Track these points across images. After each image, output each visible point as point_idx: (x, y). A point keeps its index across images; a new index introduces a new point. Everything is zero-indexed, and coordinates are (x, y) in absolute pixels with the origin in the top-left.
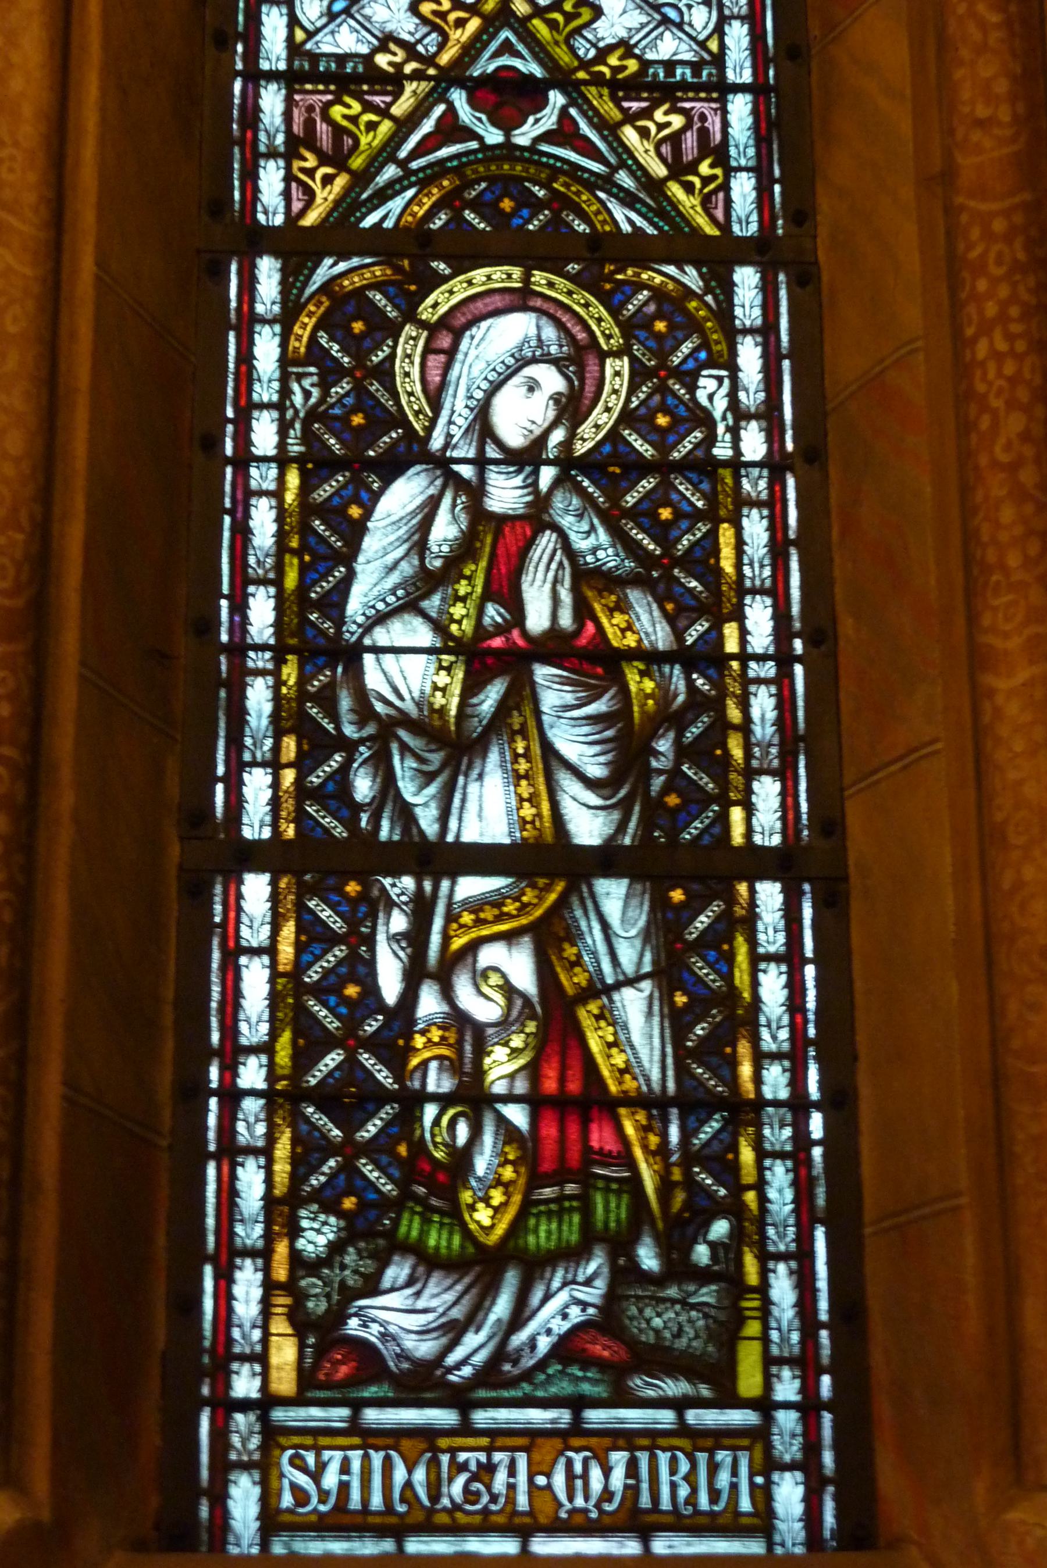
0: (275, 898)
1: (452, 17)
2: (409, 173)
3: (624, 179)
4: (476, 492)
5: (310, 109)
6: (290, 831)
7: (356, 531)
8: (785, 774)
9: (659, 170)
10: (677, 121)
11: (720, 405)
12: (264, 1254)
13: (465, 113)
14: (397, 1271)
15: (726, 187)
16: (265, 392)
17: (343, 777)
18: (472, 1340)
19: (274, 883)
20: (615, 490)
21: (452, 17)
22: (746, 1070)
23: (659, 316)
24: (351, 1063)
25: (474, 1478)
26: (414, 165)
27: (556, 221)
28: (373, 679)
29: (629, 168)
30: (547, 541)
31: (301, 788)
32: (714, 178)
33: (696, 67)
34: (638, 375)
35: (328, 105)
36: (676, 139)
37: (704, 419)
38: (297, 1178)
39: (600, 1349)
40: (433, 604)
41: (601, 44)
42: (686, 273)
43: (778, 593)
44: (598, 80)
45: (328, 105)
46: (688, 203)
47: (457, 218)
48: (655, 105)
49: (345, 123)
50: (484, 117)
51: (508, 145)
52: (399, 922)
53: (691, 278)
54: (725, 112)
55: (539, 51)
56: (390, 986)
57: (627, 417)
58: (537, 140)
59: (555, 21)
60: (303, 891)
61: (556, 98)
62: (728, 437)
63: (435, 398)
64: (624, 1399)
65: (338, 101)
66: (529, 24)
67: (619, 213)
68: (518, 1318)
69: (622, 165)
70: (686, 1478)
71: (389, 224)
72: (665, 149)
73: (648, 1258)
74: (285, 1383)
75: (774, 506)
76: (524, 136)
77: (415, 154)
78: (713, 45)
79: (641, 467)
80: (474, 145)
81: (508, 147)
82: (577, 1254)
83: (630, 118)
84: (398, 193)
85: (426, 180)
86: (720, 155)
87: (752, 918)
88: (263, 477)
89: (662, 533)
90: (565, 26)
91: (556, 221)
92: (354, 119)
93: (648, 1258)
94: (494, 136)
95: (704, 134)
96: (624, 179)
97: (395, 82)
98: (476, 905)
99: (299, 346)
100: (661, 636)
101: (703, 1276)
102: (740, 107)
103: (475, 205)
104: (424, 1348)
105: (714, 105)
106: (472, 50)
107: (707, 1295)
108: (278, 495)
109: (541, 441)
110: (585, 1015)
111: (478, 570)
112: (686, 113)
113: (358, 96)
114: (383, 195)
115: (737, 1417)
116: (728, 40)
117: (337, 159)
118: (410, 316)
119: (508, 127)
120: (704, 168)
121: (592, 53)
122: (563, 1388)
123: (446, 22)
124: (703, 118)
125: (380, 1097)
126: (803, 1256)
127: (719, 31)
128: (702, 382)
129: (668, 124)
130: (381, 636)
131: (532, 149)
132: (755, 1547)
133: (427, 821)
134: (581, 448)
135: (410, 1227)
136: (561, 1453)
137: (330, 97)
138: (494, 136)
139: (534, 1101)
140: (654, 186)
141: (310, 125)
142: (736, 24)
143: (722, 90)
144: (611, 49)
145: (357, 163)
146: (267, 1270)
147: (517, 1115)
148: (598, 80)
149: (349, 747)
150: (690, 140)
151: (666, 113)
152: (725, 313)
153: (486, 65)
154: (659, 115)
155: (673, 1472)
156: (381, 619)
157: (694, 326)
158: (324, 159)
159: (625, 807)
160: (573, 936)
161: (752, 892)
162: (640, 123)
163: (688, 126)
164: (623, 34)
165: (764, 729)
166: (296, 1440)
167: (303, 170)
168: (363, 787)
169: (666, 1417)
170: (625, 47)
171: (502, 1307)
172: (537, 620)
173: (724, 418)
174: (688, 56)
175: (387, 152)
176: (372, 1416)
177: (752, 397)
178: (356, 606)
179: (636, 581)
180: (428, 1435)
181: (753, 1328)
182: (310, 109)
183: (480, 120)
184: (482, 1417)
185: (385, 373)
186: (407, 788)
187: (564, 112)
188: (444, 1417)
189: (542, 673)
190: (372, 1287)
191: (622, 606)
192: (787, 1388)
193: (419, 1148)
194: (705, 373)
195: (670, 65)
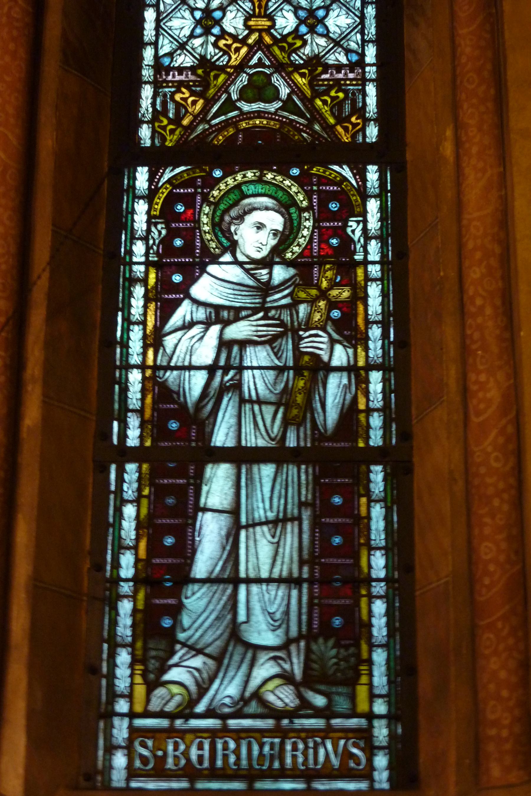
5: (165, 95)
11: (358, 233)
26: (214, 122)
35: (173, 94)
42: (343, 169)
45: (173, 94)
53: (346, 172)
59: (284, 47)
62: (362, 249)
65: (179, 91)
66: (271, 49)
72: (335, 110)
86: (361, 112)
90: (289, 49)
92: (185, 99)
113: (188, 87)
115: (353, 722)
128: (350, 224)
137: (173, 90)
141: (164, 104)
142: (370, 45)
158: (171, 121)
162: (323, 98)
163: (346, 97)
181: (364, 679)
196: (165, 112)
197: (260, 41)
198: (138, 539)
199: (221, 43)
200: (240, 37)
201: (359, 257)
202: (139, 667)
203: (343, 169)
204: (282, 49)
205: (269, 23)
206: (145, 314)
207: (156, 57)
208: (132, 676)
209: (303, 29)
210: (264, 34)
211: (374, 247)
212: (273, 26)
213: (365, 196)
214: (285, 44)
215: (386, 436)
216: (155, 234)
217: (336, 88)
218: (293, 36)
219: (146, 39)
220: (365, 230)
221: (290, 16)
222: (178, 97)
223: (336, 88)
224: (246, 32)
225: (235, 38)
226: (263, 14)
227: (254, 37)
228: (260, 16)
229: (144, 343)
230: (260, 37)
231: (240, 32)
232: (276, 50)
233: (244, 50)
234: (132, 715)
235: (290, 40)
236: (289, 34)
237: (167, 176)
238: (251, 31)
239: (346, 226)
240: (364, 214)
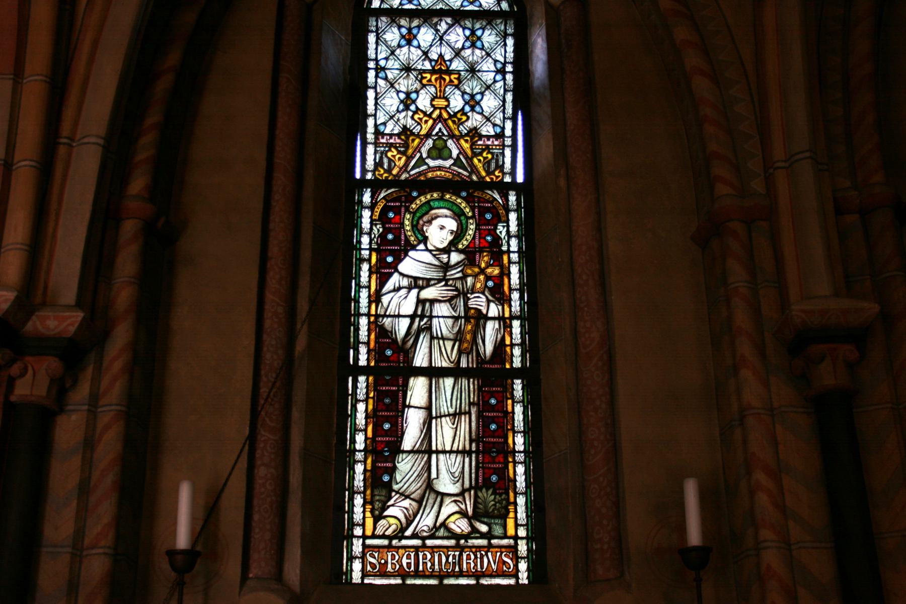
11: (504, 233)
42: (494, 193)
59: (455, 121)
62: (506, 244)
128: (499, 227)
167: (378, 174)
194: (499, 224)
197: (440, 116)
199: (416, 117)
200: (428, 113)
201: (505, 248)
202: (369, 507)
203: (494, 193)
204: (454, 122)
205: (446, 103)
206: (370, 281)
207: (376, 126)
208: (364, 512)
209: (467, 108)
211: (514, 243)
212: (448, 106)
213: (508, 210)
214: (455, 119)
215: (523, 361)
218: (461, 113)
219: (369, 112)
220: (508, 232)
221: (459, 98)
224: (432, 109)
225: (425, 113)
227: (437, 112)
229: (369, 300)
230: (441, 113)
231: (428, 109)
232: (450, 122)
233: (430, 122)
234: (364, 537)
235: (459, 116)
236: (459, 112)
238: (435, 108)
239: (496, 228)
240: (507, 221)
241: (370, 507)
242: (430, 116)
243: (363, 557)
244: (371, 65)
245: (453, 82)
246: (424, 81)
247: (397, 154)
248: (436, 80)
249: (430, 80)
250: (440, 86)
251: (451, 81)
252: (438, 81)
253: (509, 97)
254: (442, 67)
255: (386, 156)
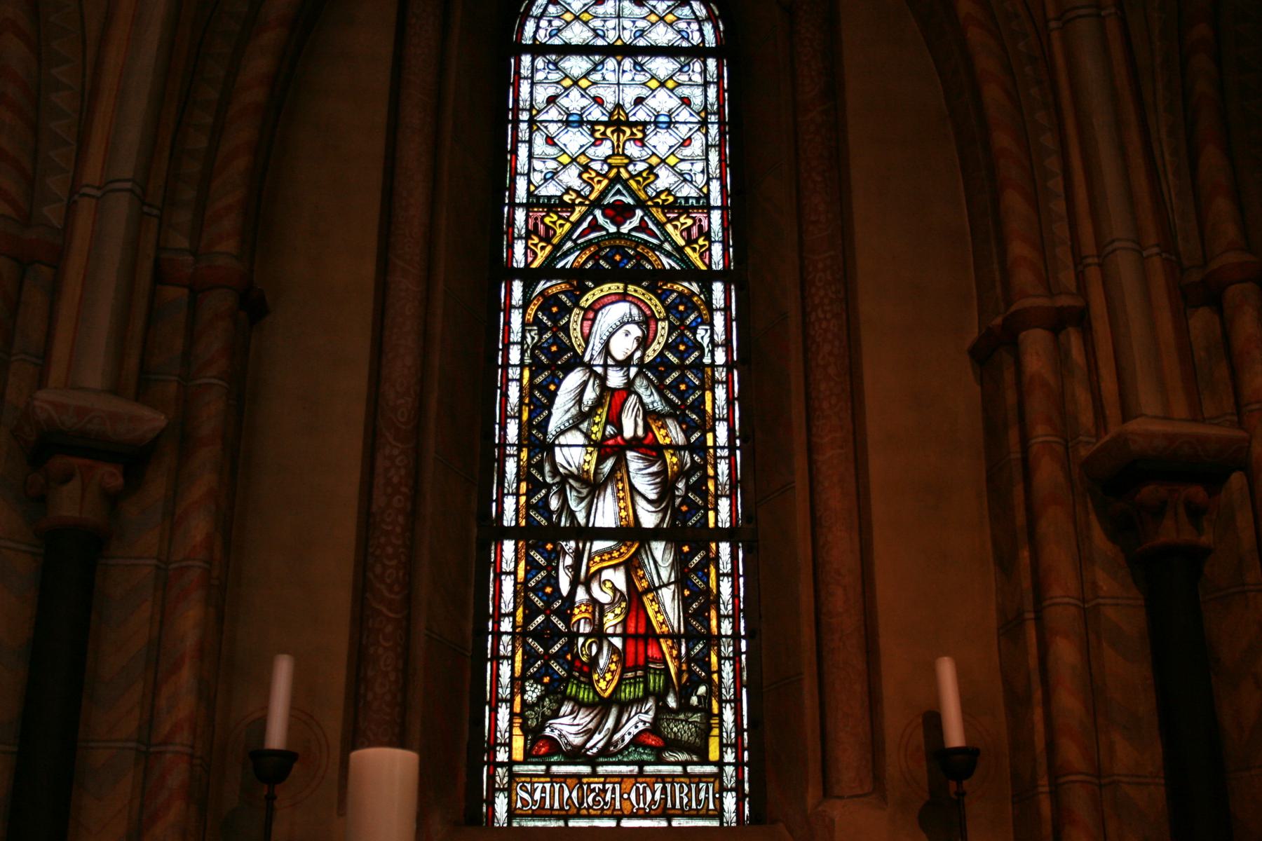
0: (516, 551)
1: (596, 180)
2: (576, 245)
3: (667, 246)
4: (603, 379)
5: (536, 219)
6: (523, 523)
7: (552, 396)
8: (732, 497)
9: (681, 242)
10: (690, 222)
11: (706, 341)
12: (511, 701)
13: (601, 220)
14: (567, 708)
15: (709, 249)
16: (516, 337)
17: (546, 500)
18: (597, 737)
19: (516, 544)
20: (661, 378)
21: (596, 180)
22: (714, 623)
23: (681, 303)
24: (548, 619)
25: (598, 795)
26: (579, 242)
27: (638, 264)
28: (559, 457)
29: (669, 242)
30: (633, 399)
31: (529, 506)
32: (705, 245)
33: (698, 199)
34: (672, 328)
35: (543, 217)
36: (689, 229)
37: (700, 347)
38: (525, 668)
39: (652, 741)
40: (584, 426)
41: (658, 190)
42: (692, 285)
43: (729, 420)
44: (656, 205)
45: (543, 217)
46: (694, 257)
47: (597, 263)
48: (680, 215)
49: (551, 224)
50: (608, 221)
51: (618, 232)
52: (569, 561)
53: (695, 288)
54: (709, 218)
55: (632, 193)
56: (565, 587)
57: (667, 346)
58: (631, 230)
60: (529, 548)
61: (639, 213)
62: (709, 354)
63: (587, 340)
64: (660, 761)
65: (548, 215)
67: (665, 260)
68: (617, 728)
69: (666, 240)
70: (686, 795)
71: (568, 266)
72: (685, 234)
73: (672, 702)
74: (518, 755)
75: (728, 383)
76: (625, 229)
77: (579, 237)
78: (705, 190)
79: (673, 367)
80: (604, 233)
81: (619, 235)
82: (641, 701)
83: (670, 221)
84: (572, 253)
85: (584, 248)
86: (708, 236)
87: (717, 558)
88: (514, 373)
89: (682, 396)
90: (643, 182)
91: (638, 264)
92: (554, 223)
93: (672, 702)
94: (612, 229)
95: (700, 227)
96: (667, 246)
97: (571, 207)
98: (601, 553)
99: (530, 318)
100: (680, 439)
101: (695, 710)
102: (716, 216)
103: (605, 258)
104: (577, 741)
105: (705, 215)
106: (604, 194)
107: (696, 718)
108: (520, 380)
109: (631, 357)
110: (646, 600)
111: (603, 412)
112: (694, 218)
113: (556, 213)
114: (566, 255)
116: (711, 188)
117: (547, 239)
118: (576, 304)
119: (618, 225)
120: (701, 241)
121: (654, 194)
122: (635, 757)
123: (593, 182)
124: (700, 220)
125: (560, 634)
126: (737, 701)
127: (707, 183)
128: (699, 331)
129: (686, 223)
130: (562, 440)
131: (629, 234)
132: (715, 823)
133: (581, 518)
134: (647, 360)
135: (571, 689)
136: (635, 784)
137: (544, 214)
138: (612, 229)
139: (624, 636)
140: (680, 249)
141: (536, 225)
142: (714, 181)
143: (708, 208)
144: (662, 192)
145: (555, 241)
146: (512, 708)
147: (617, 642)
148: (656, 205)
149: (549, 487)
150: (695, 230)
151: (685, 218)
152: (709, 303)
153: (610, 199)
154: (682, 219)
155: (681, 793)
156: (562, 432)
157: (695, 308)
158: (541, 240)
159: (664, 511)
160: (642, 566)
161: (718, 547)
162: (674, 223)
164: (667, 186)
165: (723, 478)
166: (523, 779)
167: (532, 244)
168: (554, 504)
169: (678, 769)
170: (668, 191)
171: (610, 723)
172: (628, 433)
173: (708, 346)
174: (695, 195)
175: (568, 236)
176: (555, 769)
177: (720, 336)
178: (552, 427)
179: (669, 415)
180: (579, 777)
182: (536, 219)
183: (607, 222)
184: (601, 770)
185: (566, 329)
186: (573, 504)
187: (642, 218)
188: (585, 769)
189: (630, 455)
190: (556, 715)
191: (664, 426)
192: (730, 757)
193: (576, 657)
194: (700, 327)
195: (687, 199)
196: (536, 232)
198: (515, 609)
199: (585, 176)
210: (622, 170)
216: (529, 340)
217: (685, 216)
222: (547, 220)
223: (685, 216)
226: (621, 153)
227: (615, 171)
228: (618, 154)
230: (619, 172)
232: (633, 183)
233: (605, 182)
237: (540, 288)
238: (611, 167)
241: (520, 721)
242: (605, 176)
243: (509, 790)
244: (525, 116)
245: (635, 135)
246: (598, 135)
247: (558, 219)
248: (613, 132)
249: (604, 133)
250: (618, 140)
251: (633, 134)
252: (615, 135)
253: (714, 157)
254: (621, 118)
255: (542, 222)
